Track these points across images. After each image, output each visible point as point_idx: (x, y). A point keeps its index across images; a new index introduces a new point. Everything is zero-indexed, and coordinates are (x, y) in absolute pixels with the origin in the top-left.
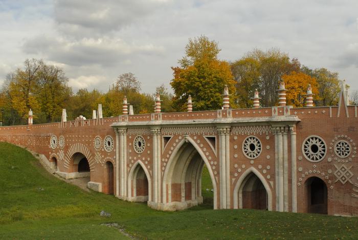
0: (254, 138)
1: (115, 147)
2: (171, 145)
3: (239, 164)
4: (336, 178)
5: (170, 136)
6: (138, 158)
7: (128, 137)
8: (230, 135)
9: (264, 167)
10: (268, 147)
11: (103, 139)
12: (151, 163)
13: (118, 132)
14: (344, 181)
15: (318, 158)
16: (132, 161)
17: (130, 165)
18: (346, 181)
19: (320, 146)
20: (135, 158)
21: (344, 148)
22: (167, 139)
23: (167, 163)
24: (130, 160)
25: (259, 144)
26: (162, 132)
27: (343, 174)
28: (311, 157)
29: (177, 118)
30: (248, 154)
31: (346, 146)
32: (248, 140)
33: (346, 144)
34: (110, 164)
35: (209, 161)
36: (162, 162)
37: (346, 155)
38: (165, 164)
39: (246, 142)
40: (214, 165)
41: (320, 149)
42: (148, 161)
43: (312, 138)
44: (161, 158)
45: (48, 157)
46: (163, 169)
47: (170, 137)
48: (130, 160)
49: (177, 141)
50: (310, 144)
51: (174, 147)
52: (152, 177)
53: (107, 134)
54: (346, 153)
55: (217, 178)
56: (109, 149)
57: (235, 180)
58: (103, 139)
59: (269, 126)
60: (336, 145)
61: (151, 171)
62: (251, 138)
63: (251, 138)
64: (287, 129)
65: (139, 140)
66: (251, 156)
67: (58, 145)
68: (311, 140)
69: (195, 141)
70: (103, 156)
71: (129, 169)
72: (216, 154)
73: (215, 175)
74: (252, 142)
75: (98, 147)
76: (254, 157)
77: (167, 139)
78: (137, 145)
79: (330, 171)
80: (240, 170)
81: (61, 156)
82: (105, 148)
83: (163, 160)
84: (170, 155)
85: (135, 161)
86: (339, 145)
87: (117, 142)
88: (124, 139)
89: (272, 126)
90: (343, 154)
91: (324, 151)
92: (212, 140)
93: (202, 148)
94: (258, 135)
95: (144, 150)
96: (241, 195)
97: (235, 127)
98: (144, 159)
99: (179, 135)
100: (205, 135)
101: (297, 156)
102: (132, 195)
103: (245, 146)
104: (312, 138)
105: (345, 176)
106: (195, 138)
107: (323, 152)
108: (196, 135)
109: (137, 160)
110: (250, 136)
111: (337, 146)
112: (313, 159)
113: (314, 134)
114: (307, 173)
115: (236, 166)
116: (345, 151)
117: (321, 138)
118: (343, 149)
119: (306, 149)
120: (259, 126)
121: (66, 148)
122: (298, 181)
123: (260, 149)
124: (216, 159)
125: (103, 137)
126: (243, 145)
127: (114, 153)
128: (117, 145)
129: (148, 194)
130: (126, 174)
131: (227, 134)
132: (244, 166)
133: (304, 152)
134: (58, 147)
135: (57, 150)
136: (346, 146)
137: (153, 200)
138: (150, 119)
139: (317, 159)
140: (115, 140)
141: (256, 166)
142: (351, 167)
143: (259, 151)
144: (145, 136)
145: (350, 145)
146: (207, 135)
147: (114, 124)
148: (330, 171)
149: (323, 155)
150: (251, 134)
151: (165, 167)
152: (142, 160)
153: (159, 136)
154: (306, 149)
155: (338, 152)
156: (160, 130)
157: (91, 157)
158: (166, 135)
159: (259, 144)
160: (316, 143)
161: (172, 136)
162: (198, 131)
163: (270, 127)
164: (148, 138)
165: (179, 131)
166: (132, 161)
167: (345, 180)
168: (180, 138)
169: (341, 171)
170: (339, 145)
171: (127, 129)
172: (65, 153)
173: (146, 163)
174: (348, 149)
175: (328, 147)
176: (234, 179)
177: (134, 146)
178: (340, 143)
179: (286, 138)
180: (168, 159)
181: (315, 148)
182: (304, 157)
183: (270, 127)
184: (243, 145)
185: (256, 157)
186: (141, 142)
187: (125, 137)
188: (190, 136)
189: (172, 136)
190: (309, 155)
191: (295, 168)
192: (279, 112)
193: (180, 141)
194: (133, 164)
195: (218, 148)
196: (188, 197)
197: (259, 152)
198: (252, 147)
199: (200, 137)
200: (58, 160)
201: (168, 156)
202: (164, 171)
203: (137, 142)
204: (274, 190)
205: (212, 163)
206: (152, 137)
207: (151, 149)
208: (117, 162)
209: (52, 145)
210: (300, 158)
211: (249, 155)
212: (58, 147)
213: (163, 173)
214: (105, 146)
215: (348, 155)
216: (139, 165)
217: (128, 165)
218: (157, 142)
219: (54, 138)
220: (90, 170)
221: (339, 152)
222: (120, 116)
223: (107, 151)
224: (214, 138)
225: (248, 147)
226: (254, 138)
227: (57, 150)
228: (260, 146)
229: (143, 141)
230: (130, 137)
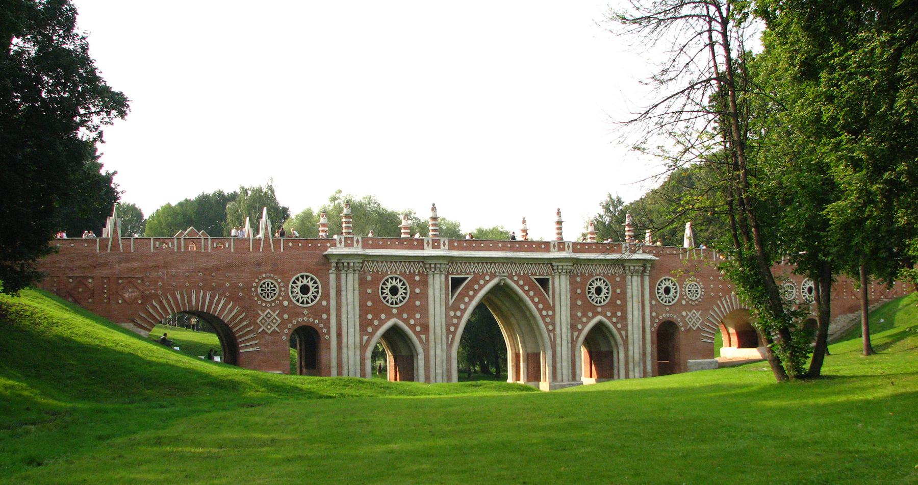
2: (464, 293)
5: (466, 276)
25: (607, 287)
62: (597, 279)
69: (516, 282)
70: (286, 316)
74: (599, 284)
94: (606, 275)
99: (484, 275)
100: (532, 274)
106: (516, 278)
114: (661, 317)
120: (600, 265)
127: (317, 311)
131: (563, 273)
146: (535, 274)
150: (597, 275)
159: (607, 287)
161: (470, 277)
162: (521, 270)
168: (487, 278)
175: (680, 289)
193: (487, 282)
218: (437, 286)
226: (600, 279)
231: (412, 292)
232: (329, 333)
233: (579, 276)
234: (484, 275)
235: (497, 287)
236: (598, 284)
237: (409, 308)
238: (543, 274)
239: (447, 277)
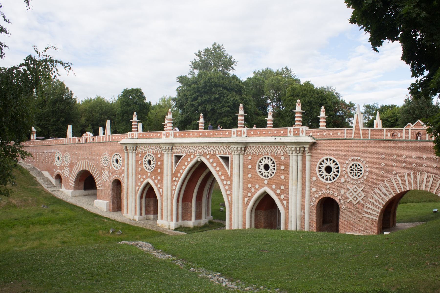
0: (269, 158)
1: (123, 165)
3: (252, 184)
4: (348, 199)
6: (147, 177)
7: (137, 154)
8: (244, 156)
9: (278, 187)
10: (283, 168)
11: (111, 156)
12: (161, 181)
13: (127, 150)
14: (355, 201)
15: (332, 178)
16: (142, 180)
17: (139, 184)
18: (357, 202)
19: (334, 167)
20: (144, 177)
21: (357, 169)
22: (178, 158)
23: (178, 182)
24: (140, 179)
25: (273, 165)
26: (174, 150)
27: (355, 194)
28: (325, 178)
29: (189, 137)
30: (262, 174)
31: (359, 167)
32: (262, 160)
33: (359, 165)
34: (117, 184)
35: (222, 181)
36: (173, 181)
37: (359, 176)
38: (176, 183)
39: (260, 162)
40: (226, 184)
41: (334, 170)
42: (159, 180)
43: (327, 160)
44: (172, 177)
45: (52, 174)
46: (174, 188)
47: (182, 156)
48: (140, 179)
49: (189, 159)
50: (325, 165)
51: (186, 166)
52: (162, 196)
53: (116, 151)
54: (359, 174)
55: (229, 197)
56: (116, 167)
57: (248, 200)
58: (111, 156)
59: (284, 146)
60: (349, 167)
61: (161, 190)
62: (265, 158)
63: (265, 158)
64: (302, 149)
65: (149, 158)
66: (265, 176)
67: (63, 162)
68: (325, 161)
69: (208, 160)
70: (111, 174)
71: (137, 188)
72: (229, 173)
73: (228, 195)
74: (267, 162)
75: (105, 165)
76: (268, 176)
77: (178, 158)
78: (147, 162)
79: (342, 192)
80: (253, 190)
81: (65, 173)
82: (113, 166)
83: (174, 179)
84: (181, 174)
85: (144, 179)
86: (353, 167)
87: (126, 160)
88: (132, 157)
89: (287, 146)
90: (356, 175)
91: (338, 172)
92: (226, 159)
93: (215, 168)
95: (153, 168)
96: (253, 215)
97: (250, 146)
98: (153, 177)
99: (191, 154)
100: (219, 154)
101: (311, 177)
102: (141, 214)
103: (259, 166)
104: (327, 160)
105: (357, 196)
107: (336, 173)
108: (210, 154)
109: (146, 178)
110: (265, 156)
111: (351, 167)
112: (327, 179)
113: (329, 155)
115: (249, 186)
116: (358, 172)
117: (335, 160)
118: (356, 170)
119: (320, 169)
121: (71, 166)
122: (311, 200)
123: (274, 169)
124: (229, 178)
125: (110, 154)
126: (257, 165)
127: (121, 172)
128: (126, 163)
129: (157, 213)
130: (134, 192)
132: (257, 186)
133: (318, 173)
134: (63, 164)
135: (62, 167)
136: (359, 167)
137: (162, 218)
138: (160, 137)
139: (330, 180)
140: (124, 158)
141: (269, 185)
142: (362, 188)
143: (273, 171)
144: (156, 154)
145: (362, 167)
146: (220, 154)
147: (123, 141)
148: (342, 192)
149: (336, 175)
150: (265, 154)
151: (176, 186)
152: (152, 179)
153: (170, 154)
154: (320, 169)
155: (351, 173)
156: (172, 148)
157: (97, 174)
158: (177, 153)
159: (273, 165)
160: (331, 164)
161: (184, 155)
162: (211, 150)
163: (285, 147)
164: (159, 156)
165: (192, 150)
166: (142, 180)
167: (357, 200)
168: (192, 156)
169: (353, 191)
170: (353, 167)
171: (137, 146)
172: (71, 170)
173: (156, 181)
174: (361, 171)
175: (342, 168)
176: (246, 199)
177: (143, 164)
178: (353, 165)
179: (300, 158)
180: (179, 178)
181: (328, 170)
182: (318, 179)
183: (285, 147)
184: (257, 165)
185: (270, 177)
186: (151, 160)
187: (134, 155)
188: (203, 155)
189: (184, 155)
190: (323, 176)
191: (307, 189)
192: (294, 132)
193: (192, 159)
194: (142, 183)
195: (232, 167)
196: (198, 216)
197: (273, 173)
198: (267, 167)
199: (213, 156)
200: (63, 178)
201: (179, 175)
202: (175, 190)
203: (147, 160)
204: (287, 209)
205: (225, 182)
206: (162, 155)
207: (161, 167)
208: (126, 180)
209: (57, 163)
210: (314, 179)
211: (264, 175)
212: (63, 164)
213: (173, 192)
214: (112, 164)
215: (361, 176)
216: (148, 183)
217: (136, 185)
219: (58, 155)
220: (96, 188)
221: (352, 174)
222: (129, 133)
223: (114, 168)
224: (228, 157)
225: (262, 167)
226: (269, 158)
227: (62, 167)
228: (274, 166)
229: (153, 159)
230: (140, 155)
231: (157, 164)
232: (124, 183)
233: (251, 155)
234: (191, 154)
235: (197, 161)
236: (267, 162)
237: (155, 172)
238: (226, 154)
239: (172, 156)
